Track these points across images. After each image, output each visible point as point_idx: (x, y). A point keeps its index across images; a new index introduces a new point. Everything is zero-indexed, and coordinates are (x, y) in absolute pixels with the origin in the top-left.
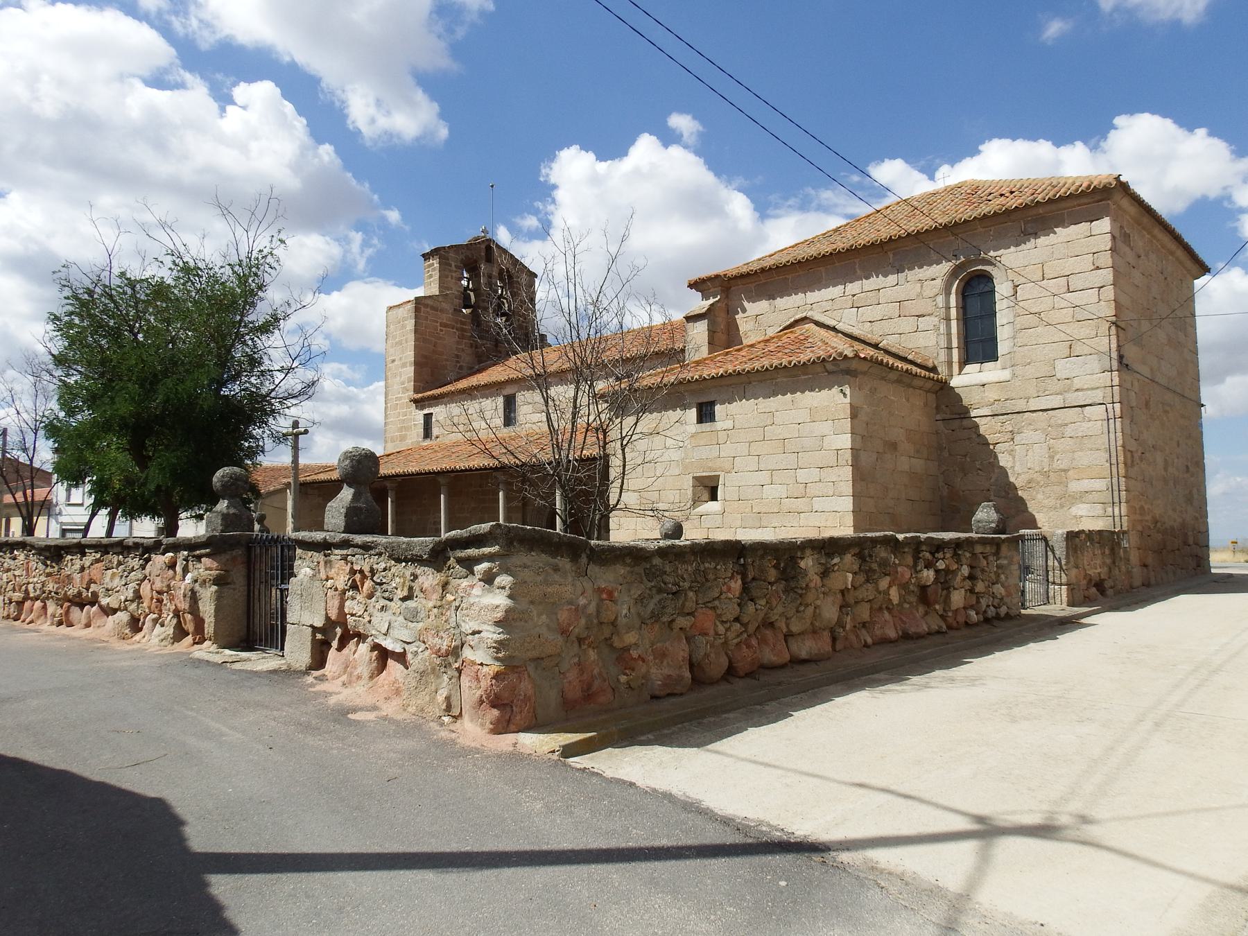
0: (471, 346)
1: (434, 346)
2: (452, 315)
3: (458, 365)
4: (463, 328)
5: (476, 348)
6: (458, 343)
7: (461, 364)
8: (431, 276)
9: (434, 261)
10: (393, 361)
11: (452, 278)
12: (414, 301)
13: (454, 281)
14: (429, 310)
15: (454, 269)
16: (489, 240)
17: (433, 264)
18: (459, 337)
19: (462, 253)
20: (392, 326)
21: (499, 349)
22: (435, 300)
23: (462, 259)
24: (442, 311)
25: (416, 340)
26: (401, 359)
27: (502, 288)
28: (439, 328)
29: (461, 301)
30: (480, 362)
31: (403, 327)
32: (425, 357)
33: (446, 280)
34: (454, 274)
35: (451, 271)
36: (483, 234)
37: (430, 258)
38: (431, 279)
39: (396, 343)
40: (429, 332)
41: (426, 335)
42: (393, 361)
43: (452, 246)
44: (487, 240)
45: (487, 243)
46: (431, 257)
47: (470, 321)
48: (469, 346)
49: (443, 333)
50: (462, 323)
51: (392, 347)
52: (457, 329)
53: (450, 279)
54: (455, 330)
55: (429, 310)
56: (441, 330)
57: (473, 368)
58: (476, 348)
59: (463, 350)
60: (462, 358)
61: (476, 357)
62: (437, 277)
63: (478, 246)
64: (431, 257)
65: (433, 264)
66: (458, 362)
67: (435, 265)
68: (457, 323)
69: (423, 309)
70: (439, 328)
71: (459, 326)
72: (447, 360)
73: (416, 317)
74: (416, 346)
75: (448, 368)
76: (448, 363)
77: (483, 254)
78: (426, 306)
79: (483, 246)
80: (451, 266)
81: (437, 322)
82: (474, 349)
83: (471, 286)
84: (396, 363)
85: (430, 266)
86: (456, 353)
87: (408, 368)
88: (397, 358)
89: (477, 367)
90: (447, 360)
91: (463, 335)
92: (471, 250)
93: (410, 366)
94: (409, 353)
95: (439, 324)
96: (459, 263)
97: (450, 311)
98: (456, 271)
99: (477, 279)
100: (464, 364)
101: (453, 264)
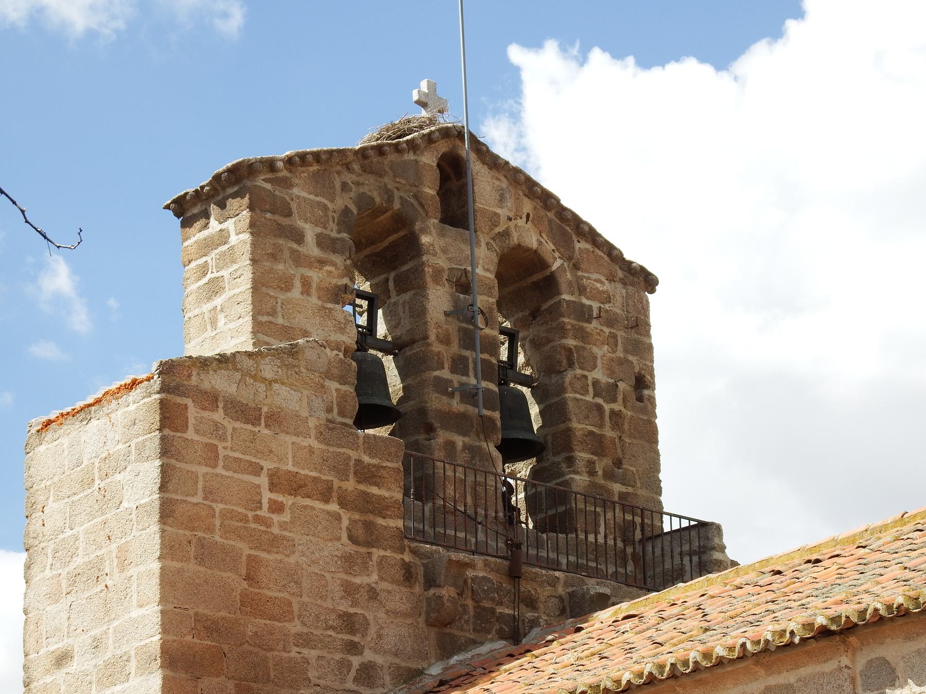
0: (408, 575)
1: (248, 578)
2: (320, 437)
3: (356, 661)
4: (365, 496)
5: (430, 582)
6: (348, 561)
7: (369, 656)
8: (214, 288)
9: (230, 224)
10: (62, 659)
11: (306, 290)
12: (157, 383)
13: (314, 300)
14: (218, 416)
15: (316, 252)
16: (454, 134)
17: (223, 238)
18: (350, 538)
19: (344, 186)
20: (52, 506)
21: (526, 587)
22: (246, 373)
23: (346, 211)
24: (275, 419)
25: (169, 550)
26: (97, 645)
27: (512, 336)
28: (267, 496)
29: (350, 389)
30: (447, 648)
31: (108, 499)
32: (210, 628)
33: (282, 296)
34: (315, 275)
35: (298, 259)
36: (424, 113)
37: (207, 216)
38: (218, 301)
39: (74, 578)
40: (223, 515)
41: (210, 529)
42: (62, 659)
43: (303, 156)
44: (446, 133)
45: (443, 147)
46: (214, 209)
47: (398, 465)
48: (399, 576)
49: (286, 517)
50: (367, 475)
51: (54, 597)
52: (342, 504)
53: (296, 293)
54: (334, 507)
55: (218, 416)
56: (277, 508)
57: (420, 673)
58: (430, 582)
59: (373, 593)
60: (372, 631)
61: (430, 624)
62: (245, 284)
63: (410, 156)
64: (214, 209)
65: (223, 238)
66: (353, 648)
67: (234, 239)
68: (344, 476)
69: (193, 413)
70: (267, 496)
71: (350, 485)
72: (305, 641)
73: (166, 449)
74: (168, 581)
75: (312, 674)
76: (314, 653)
77: (430, 190)
78: (210, 399)
79: (429, 159)
80: (299, 237)
81: (257, 470)
82: (418, 589)
83: (382, 330)
84: (74, 667)
85: (208, 246)
86: (344, 606)
87: (134, 681)
88: (79, 643)
89: (436, 670)
90: (305, 641)
91: (369, 526)
92: (380, 174)
93: (143, 669)
94: (136, 613)
95: (263, 481)
96: (333, 226)
97: (312, 422)
98: (322, 262)
99: (407, 296)
100: (379, 660)
101: (310, 232)
